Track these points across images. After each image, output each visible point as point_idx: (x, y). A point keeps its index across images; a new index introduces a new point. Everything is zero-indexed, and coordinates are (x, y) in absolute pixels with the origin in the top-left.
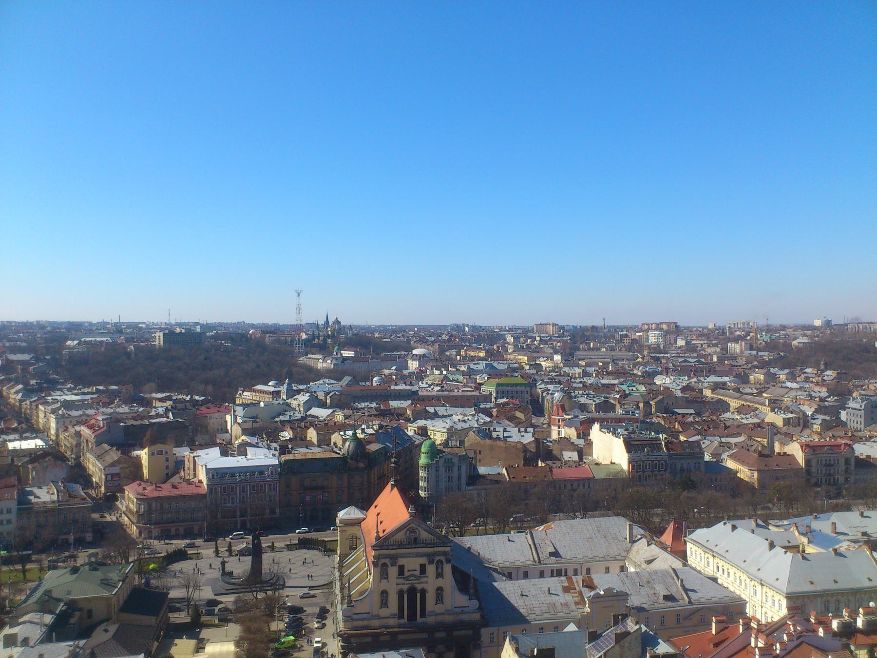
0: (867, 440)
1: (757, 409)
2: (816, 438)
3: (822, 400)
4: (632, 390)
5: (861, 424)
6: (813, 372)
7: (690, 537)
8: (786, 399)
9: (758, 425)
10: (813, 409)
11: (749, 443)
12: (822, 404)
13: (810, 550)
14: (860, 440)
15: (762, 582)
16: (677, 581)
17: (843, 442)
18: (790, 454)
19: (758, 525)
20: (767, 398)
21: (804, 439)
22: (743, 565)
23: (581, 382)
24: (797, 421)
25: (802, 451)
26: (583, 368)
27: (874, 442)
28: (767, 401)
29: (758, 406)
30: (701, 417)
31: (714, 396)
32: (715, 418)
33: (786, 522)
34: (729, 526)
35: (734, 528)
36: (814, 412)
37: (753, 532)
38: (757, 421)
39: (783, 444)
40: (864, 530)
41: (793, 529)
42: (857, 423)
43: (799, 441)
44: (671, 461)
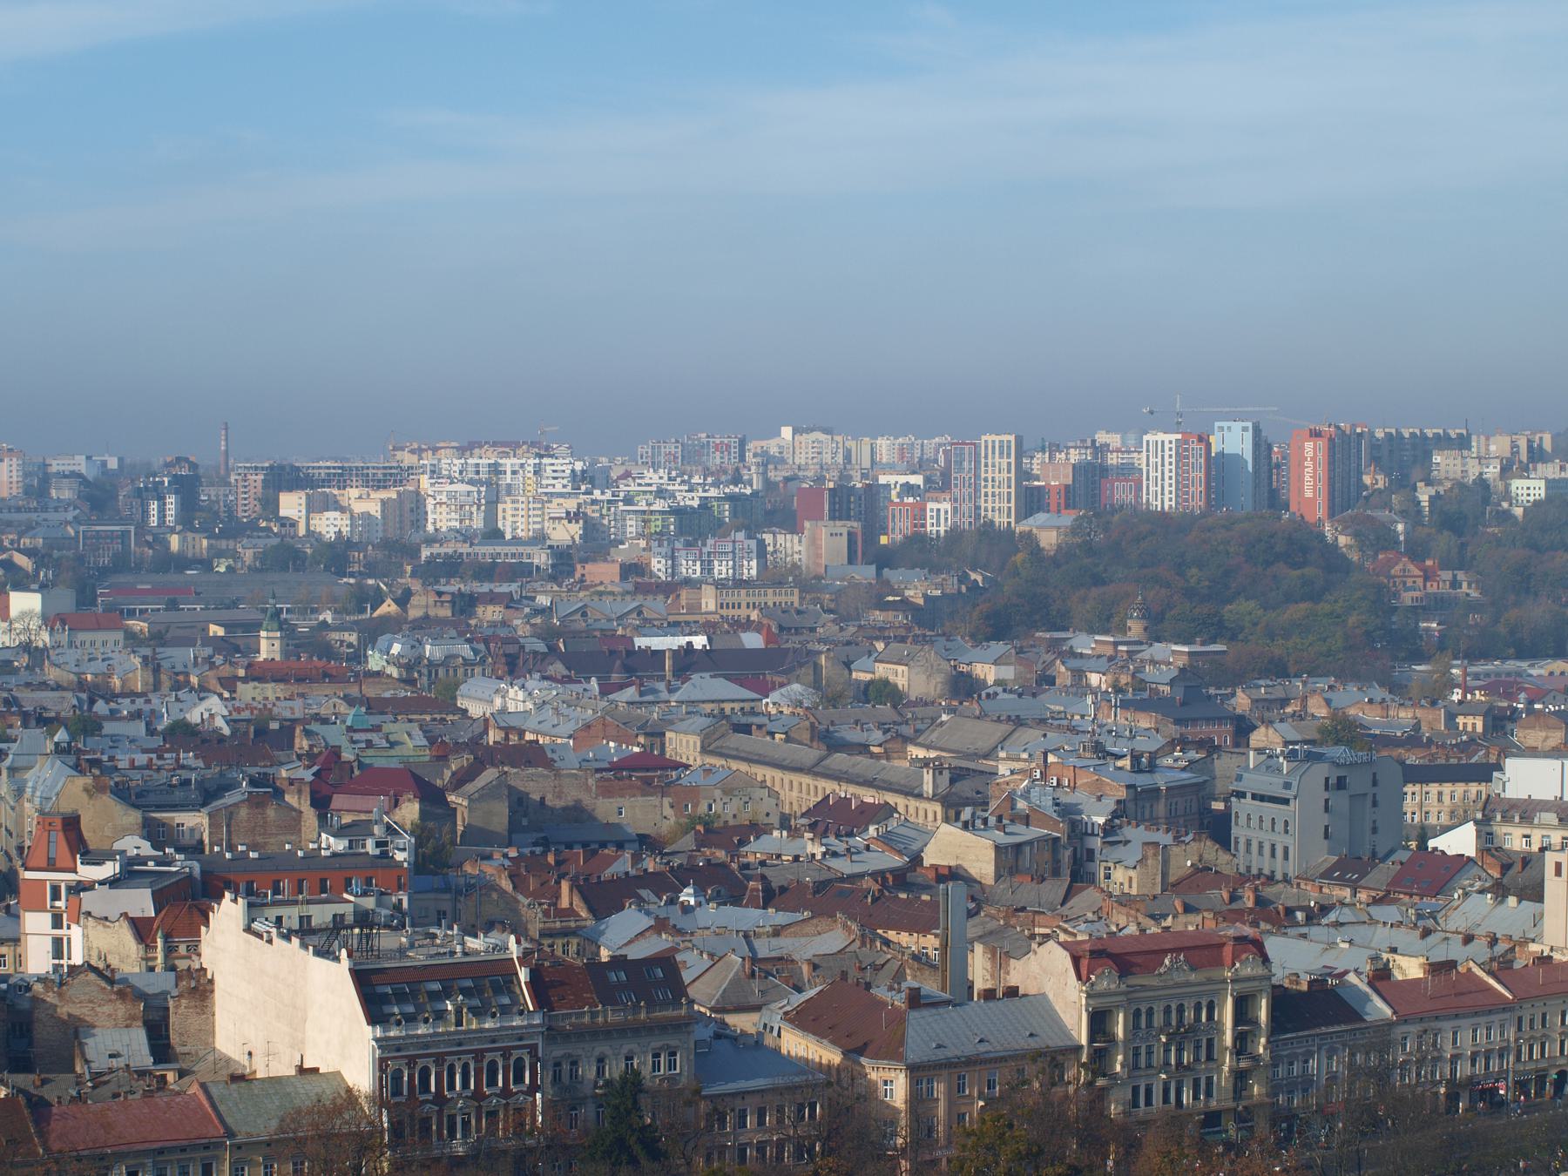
0: (1311, 918)
1: (888, 811)
2: (1126, 925)
4: (369, 744)
6: (1101, 650)
8: (1003, 769)
9: (901, 879)
12: (1142, 780)
14: (1284, 919)
17: (1231, 932)
18: (1032, 991)
20: (925, 763)
21: (1083, 926)
23: (136, 715)
24: (1047, 855)
25: (1079, 978)
26: (147, 652)
27: (1338, 924)
28: (928, 777)
29: (891, 798)
30: (663, 855)
31: (718, 762)
32: (721, 855)
36: (1115, 815)
38: (897, 861)
42: (1273, 855)
43: (1063, 937)
44: (558, 1052)
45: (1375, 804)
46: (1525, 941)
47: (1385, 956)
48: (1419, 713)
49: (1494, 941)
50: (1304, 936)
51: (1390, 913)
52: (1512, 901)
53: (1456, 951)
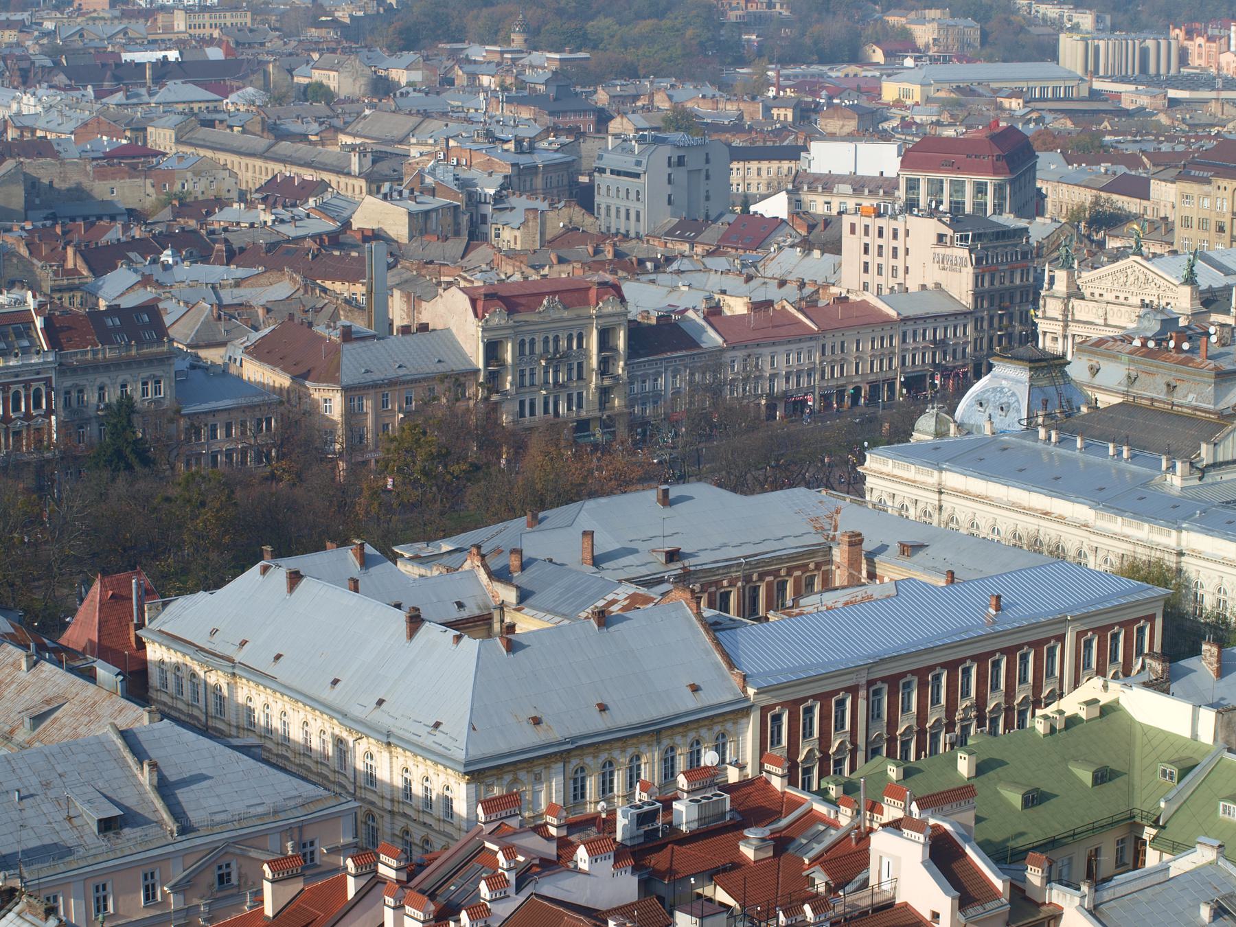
0: (657, 268)
1: (323, 186)
2: (513, 274)
3: (525, 147)
5: (638, 219)
6: (491, 57)
7: (154, 626)
8: (414, 152)
9: (333, 240)
10: (498, 179)
11: (310, 302)
12: (524, 160)
13: (527, 623)
14: (637, 268)
15: (391, 740)
16: (135, 768)
17: (595, 279)
18: (439, 327)
19: (366, 562)
20: (353, 148)
21: (479, 275)
22: (328, 695)
24: (450, 219)
25: (476, 315)
27: (679, 272)
28: (355, 159)
29: (326, 176)
30: (147, 224)
31: (189, 150)
32: (193, 223)
33: (446, 547)
34: (279, 576)
35: (295, 578)
36: (503, 187)
37: (355, 586)
38: (331, 226)
39: (414, 301)
40: (670, 545)
41: (471, 563)
42: (628, 218)
43: (463, 284)
44: (68, 383)
45: (707, 177)
46: (827, 285)
47: (717, 297)
48: (742, 106)
49: (802, 285)
50: (653, 281)
51: (720, 263)
52: (816, 253)
53: (772, 292)
